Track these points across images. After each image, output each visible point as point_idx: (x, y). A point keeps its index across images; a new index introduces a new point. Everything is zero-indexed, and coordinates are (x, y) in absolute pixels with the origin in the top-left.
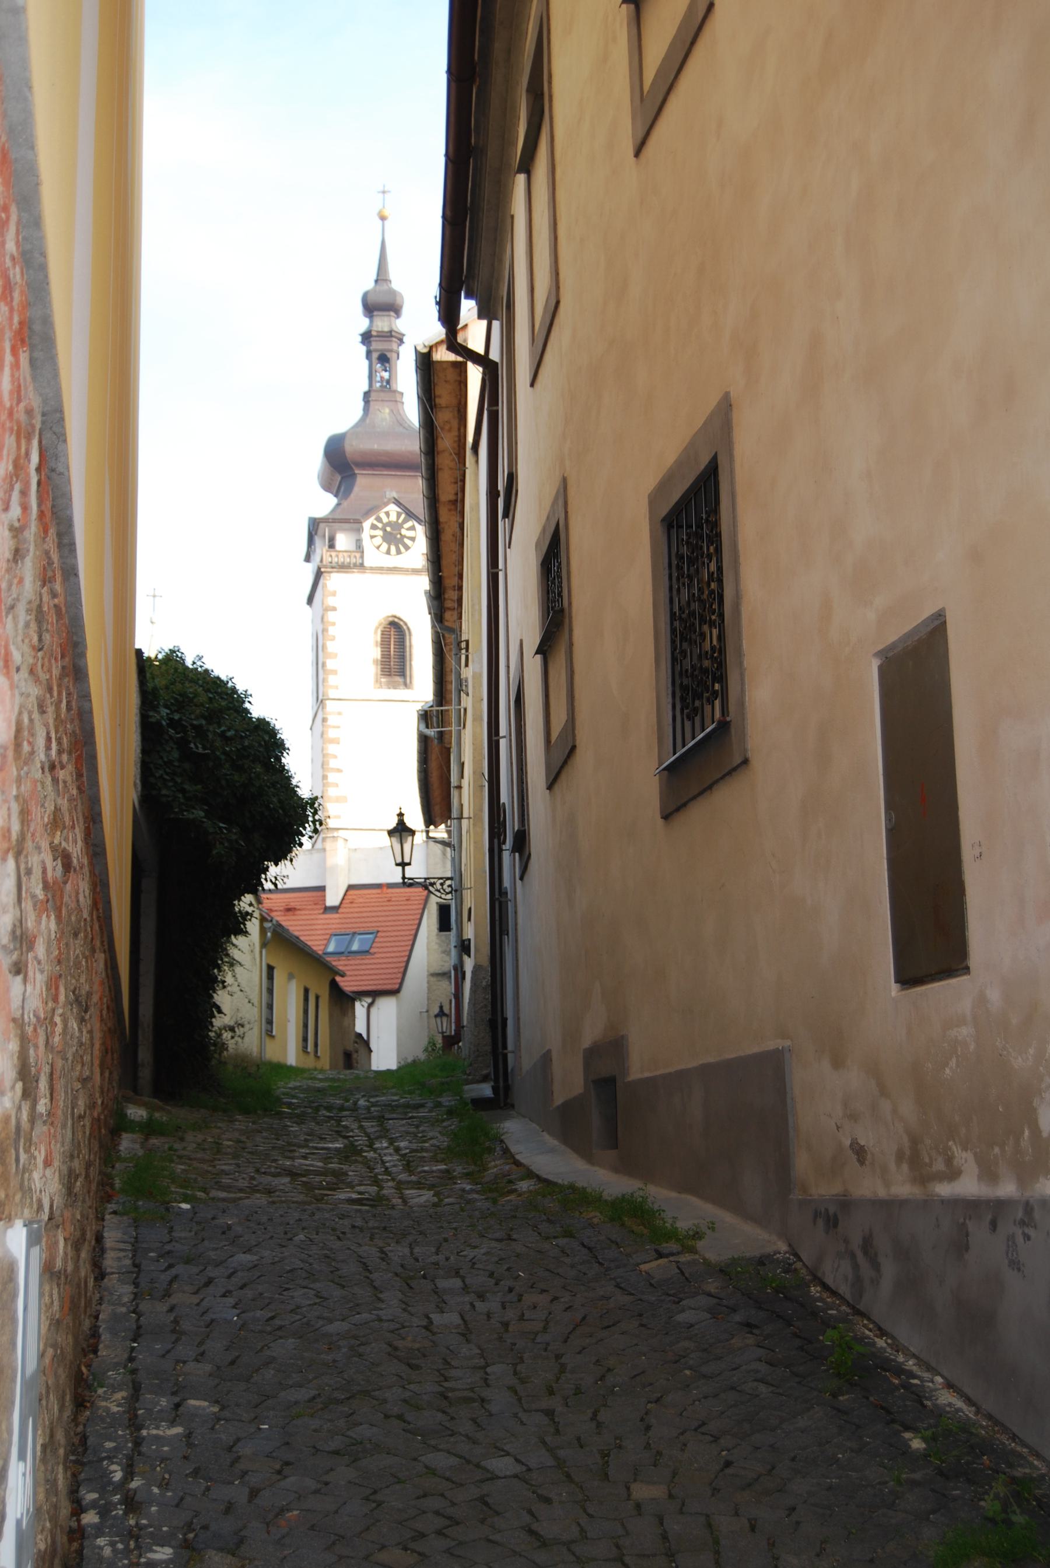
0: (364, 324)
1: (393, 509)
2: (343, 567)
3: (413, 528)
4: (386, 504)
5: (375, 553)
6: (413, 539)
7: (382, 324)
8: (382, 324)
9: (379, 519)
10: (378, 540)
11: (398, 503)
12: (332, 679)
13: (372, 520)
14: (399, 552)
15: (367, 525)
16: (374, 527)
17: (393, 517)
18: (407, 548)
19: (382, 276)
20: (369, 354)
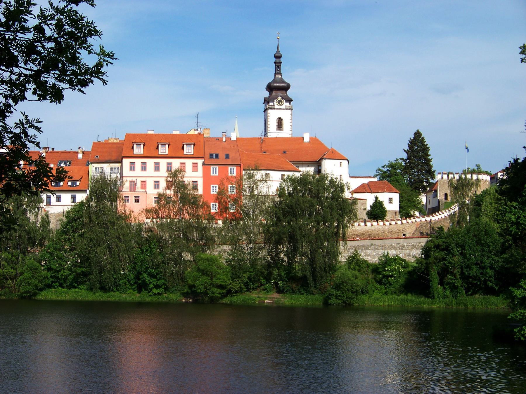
0: (274, 60)
1: (280, 97)
2: (271, 109)
3: (283, 101)
4: (279, 97)
5: (276, 106)
6: (283, 103)
7: (278, 60)
8: (278, 60)
9: (277, 99)
10: (277, 103)
11: (281, 96)
12: (269, 129)
13: (276, 100)
14: (281, 105)
15: (275, 101)
16: (276, 101)
17: (280, 99)
18: (282, 105)
19: (278, 49)
20: (275, 66)
